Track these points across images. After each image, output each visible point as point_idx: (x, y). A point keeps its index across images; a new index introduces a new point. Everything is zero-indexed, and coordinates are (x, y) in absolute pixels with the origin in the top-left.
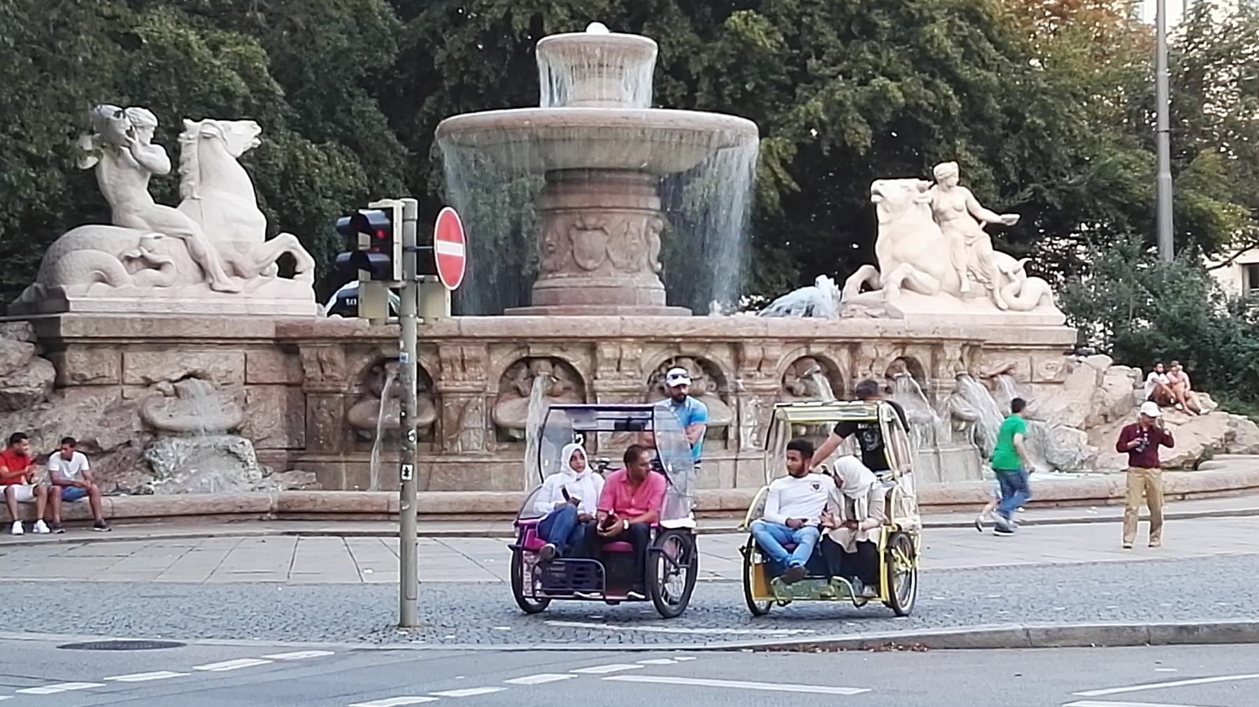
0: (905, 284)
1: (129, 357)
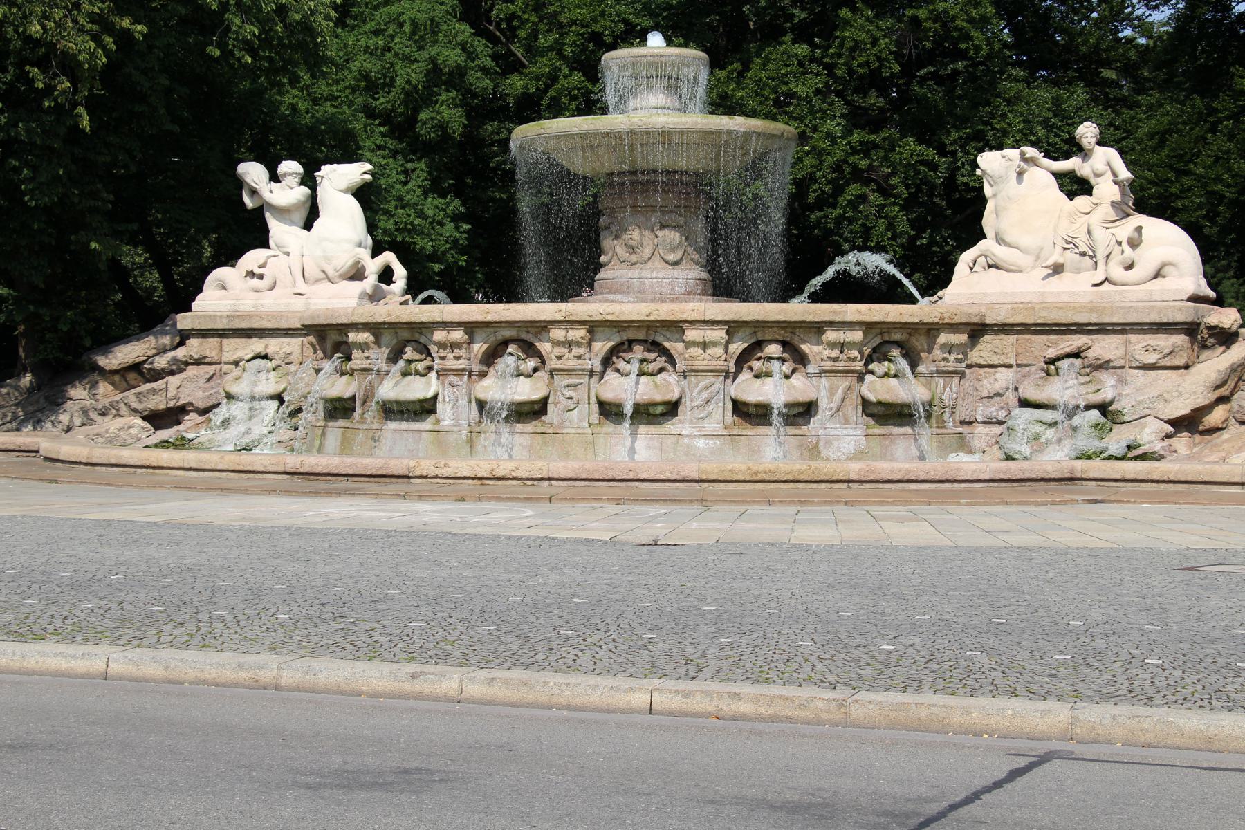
1: (225, 341)
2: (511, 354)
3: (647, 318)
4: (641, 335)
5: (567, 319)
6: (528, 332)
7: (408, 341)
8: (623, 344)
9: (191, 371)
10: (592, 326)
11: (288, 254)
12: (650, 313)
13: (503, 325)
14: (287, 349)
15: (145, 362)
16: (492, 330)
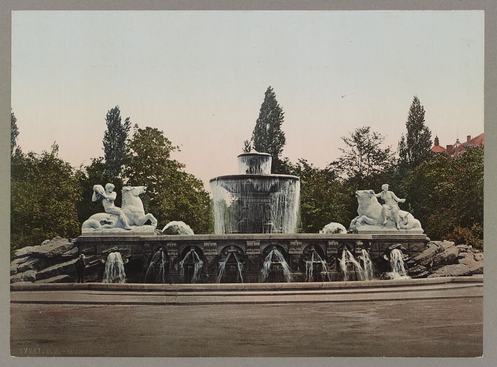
0: (364, 222)
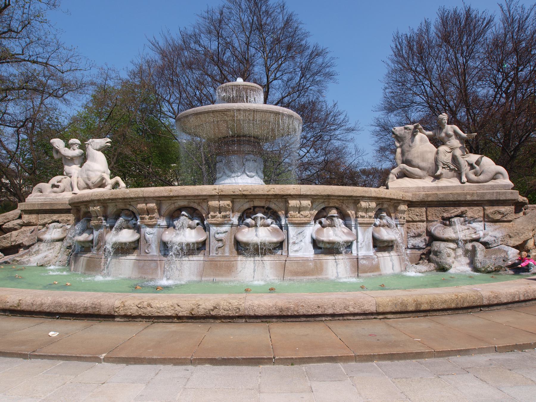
2: (183, 215)
3: (267, 193)
4: (262, 204)
5: (219, 194)
6: (194, 202)
7: (123, 210)
8: (250, 209)
9: (24, 228)
10: (233, 199)
11: (71, 177)
12: (269, 190)
13: (180, 198)
14: (69, 218)
15: (3, 225)
16: (173, 201)
